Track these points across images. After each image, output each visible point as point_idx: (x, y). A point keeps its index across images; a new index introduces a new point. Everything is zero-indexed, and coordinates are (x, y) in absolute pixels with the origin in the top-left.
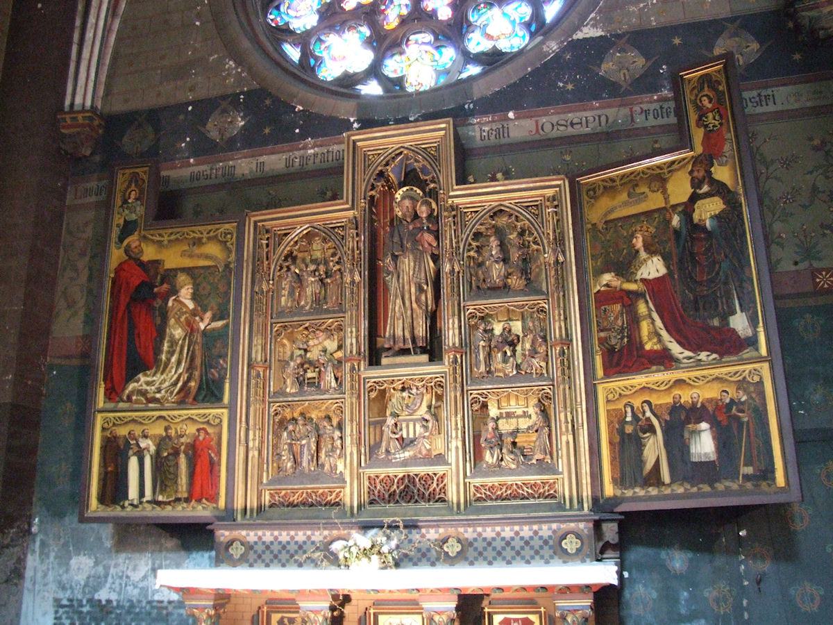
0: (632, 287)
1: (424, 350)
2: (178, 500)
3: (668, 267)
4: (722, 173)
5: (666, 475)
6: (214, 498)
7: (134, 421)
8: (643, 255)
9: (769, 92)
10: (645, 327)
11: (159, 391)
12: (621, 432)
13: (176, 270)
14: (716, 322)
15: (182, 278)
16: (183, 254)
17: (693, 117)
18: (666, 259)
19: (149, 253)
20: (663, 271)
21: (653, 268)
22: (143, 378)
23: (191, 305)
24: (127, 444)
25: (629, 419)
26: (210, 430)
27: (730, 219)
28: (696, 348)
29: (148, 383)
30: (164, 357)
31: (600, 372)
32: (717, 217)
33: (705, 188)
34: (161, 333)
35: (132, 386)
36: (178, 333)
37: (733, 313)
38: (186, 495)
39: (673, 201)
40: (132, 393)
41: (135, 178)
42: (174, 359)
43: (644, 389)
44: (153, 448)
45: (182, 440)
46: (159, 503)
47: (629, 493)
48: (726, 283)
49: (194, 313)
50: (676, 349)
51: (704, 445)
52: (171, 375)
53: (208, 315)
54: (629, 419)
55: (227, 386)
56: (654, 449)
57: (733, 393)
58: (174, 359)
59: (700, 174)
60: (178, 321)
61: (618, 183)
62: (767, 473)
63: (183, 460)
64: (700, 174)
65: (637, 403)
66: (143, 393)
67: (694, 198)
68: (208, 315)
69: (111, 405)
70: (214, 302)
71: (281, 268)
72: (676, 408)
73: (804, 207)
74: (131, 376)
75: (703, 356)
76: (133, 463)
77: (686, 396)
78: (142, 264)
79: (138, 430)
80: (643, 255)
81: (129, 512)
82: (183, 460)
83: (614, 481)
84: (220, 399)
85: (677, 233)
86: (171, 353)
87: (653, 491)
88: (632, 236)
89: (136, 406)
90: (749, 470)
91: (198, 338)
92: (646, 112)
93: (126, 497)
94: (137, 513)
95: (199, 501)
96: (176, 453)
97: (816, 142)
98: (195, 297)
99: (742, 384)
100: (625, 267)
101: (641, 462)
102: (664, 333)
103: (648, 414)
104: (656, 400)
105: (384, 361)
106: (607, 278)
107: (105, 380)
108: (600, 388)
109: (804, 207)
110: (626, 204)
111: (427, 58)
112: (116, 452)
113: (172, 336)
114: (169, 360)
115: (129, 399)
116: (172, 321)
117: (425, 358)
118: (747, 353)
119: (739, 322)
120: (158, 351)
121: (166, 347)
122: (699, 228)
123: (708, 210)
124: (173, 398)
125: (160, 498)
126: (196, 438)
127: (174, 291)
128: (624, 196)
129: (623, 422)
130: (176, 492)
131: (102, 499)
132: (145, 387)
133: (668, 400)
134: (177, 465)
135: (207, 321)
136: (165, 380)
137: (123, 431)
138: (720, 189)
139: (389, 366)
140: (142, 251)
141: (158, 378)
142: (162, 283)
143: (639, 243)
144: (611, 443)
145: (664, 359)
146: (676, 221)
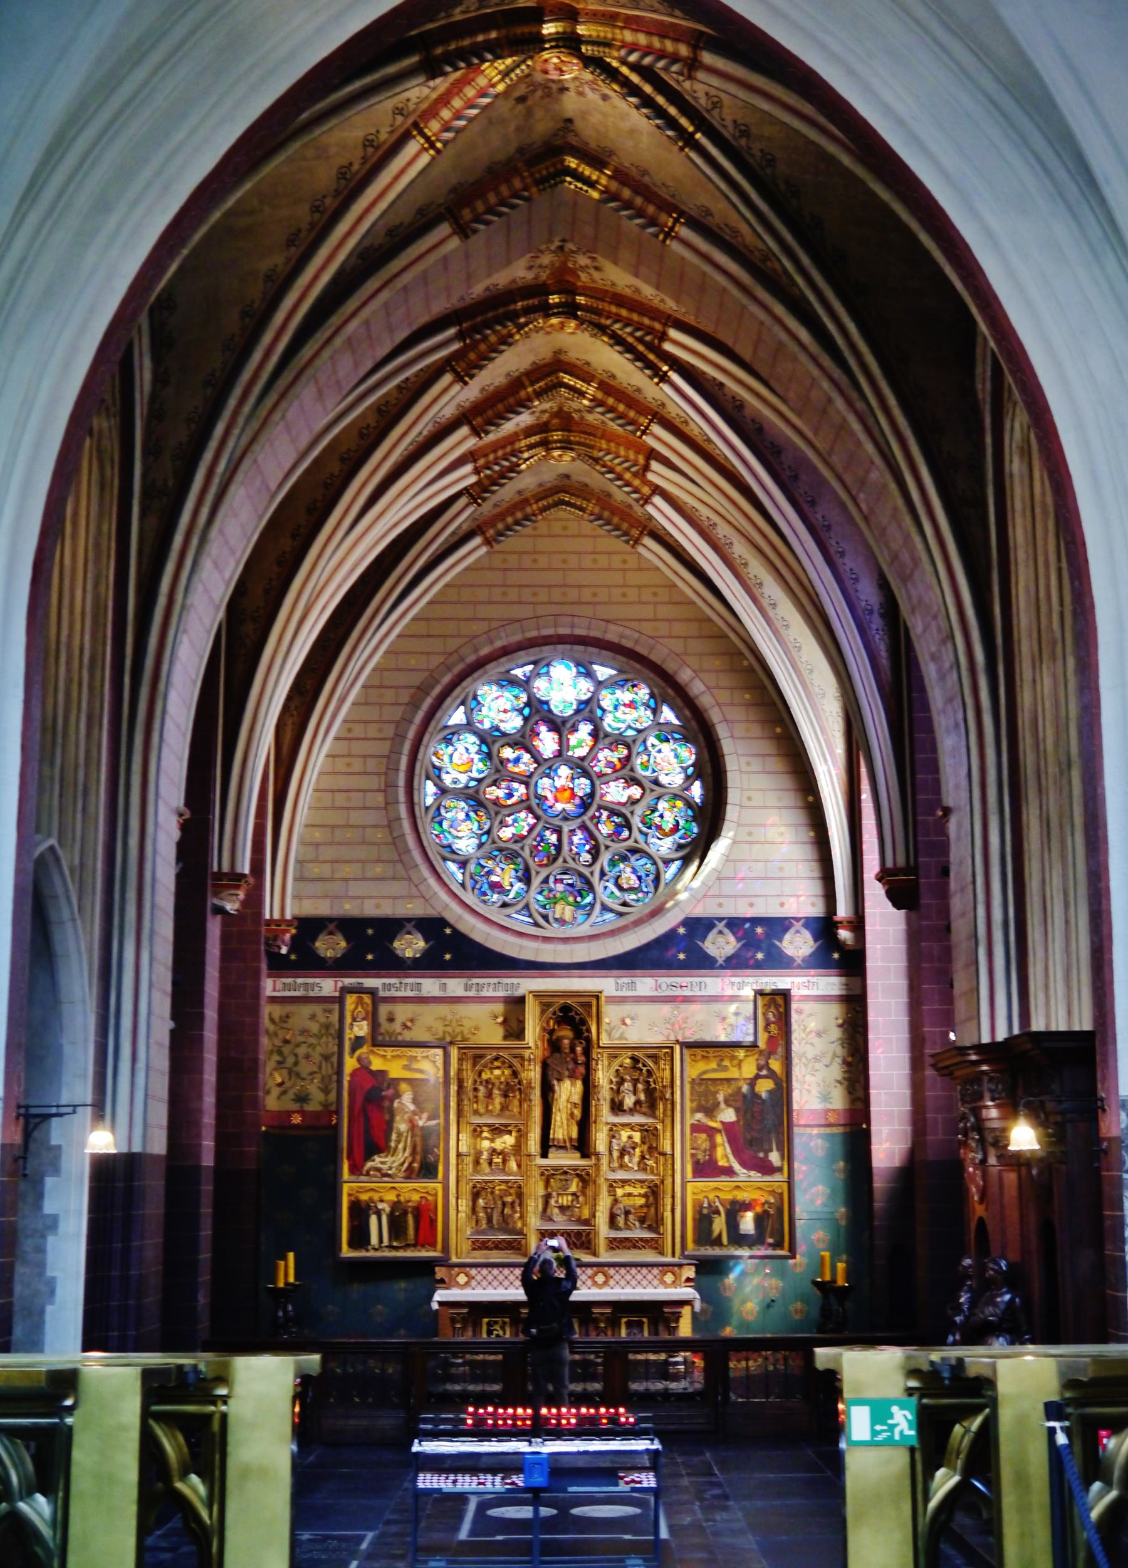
1: (576, 1148)
3: (737, 1116)
5: (725, 1240)
7: (372, 1190)
8: (722, 1105)
9: (815, 979)
10: (720, 1152)
11: (390, 1168)
12: (700, 1212)
13: (398, 1081)
14: (761, 1155)
15: (403, 1086)
16: (406, 1068)
18: (737, 1110)
19: (377, 1064)
21: (729, 1115)
22: (377, 1161)
23: (412, 1107)
24: (368, 1207)
25: (705, 1205)
26: (430, 1198)
29: (382, 1163)
30: (393, 1144)
32: (770, 1092)
33: (764, 1072)
35: (369, 1164)
37: (771, 1150)
38: (412, 1242)
41: (360, 1002)
42: (401, 1146)
43: (717, 1189)
44: (388, 1209)
45: (410, 1204)
48: (769, 1133)
49: (414, 1113)
52: (400, 1157)
53: (425, 1115)
54: (705, 1205)
56: (719, 1225)
58: (401, 1146)
59: (762, 1062)
61: (711, 1055)
65: (711, 1196)
66: (378, 1170)
67: (757, 1077)
68: (425, 1115)
69: (353, 1178)
71: (475, 1081)
72: (734, 1202)
73: (827, 1066)
74: (368, 1156)
76: (373, 1220)
78: (372, 1072)
79: (376, 1197)
80: (722, 1105)
81: (371, 1254)
84: (435, 1176)
85: (744, 1096)
86: (398, 1142)
88: (717, 1092)
89: (374, 1179)
92: (733, 984)
93: (368, 1242)
94: (378, 1254)
95: (423, 1246)
96: (405, 1213)
98: (415, 1101)
100: (710, 1110)
101: (710, 1231)
102: (731, 1157)
103: (718, 1204)
104: (723, 1196)
105: (550, 1155)
106: (699, 1116)
107: (349, 1158)
108: (689, 1184)
109: (827, 1066)
110: (714, 1070)
111: (571, 899)
112: (360, 1211)
113: (398, 1130)
114: (397, 1147)
120: (388, 1139)
121: (394, 1136)
122: (758, 1096)
124: (402, 1174)
125: (395, 1244)
126: (420, 1203)
127: (398, 1095)
128: (714, 1065)
129: (702, 1207)
130: (406, 1240)
131: (352, 1245)
132: (380, 1165)
133: (729, 1197)
134: (406, 1222)
135: (424, 1120)
136: (394, 1162)
137: (364, 1197)
138: (772, 1075)
140: (370, 1063)
141: (389, 1159)
142: (388, 1087)
143: (721, 1097)
144: (694, 1219)
145: (729, 1171)
146: (745, 1089)
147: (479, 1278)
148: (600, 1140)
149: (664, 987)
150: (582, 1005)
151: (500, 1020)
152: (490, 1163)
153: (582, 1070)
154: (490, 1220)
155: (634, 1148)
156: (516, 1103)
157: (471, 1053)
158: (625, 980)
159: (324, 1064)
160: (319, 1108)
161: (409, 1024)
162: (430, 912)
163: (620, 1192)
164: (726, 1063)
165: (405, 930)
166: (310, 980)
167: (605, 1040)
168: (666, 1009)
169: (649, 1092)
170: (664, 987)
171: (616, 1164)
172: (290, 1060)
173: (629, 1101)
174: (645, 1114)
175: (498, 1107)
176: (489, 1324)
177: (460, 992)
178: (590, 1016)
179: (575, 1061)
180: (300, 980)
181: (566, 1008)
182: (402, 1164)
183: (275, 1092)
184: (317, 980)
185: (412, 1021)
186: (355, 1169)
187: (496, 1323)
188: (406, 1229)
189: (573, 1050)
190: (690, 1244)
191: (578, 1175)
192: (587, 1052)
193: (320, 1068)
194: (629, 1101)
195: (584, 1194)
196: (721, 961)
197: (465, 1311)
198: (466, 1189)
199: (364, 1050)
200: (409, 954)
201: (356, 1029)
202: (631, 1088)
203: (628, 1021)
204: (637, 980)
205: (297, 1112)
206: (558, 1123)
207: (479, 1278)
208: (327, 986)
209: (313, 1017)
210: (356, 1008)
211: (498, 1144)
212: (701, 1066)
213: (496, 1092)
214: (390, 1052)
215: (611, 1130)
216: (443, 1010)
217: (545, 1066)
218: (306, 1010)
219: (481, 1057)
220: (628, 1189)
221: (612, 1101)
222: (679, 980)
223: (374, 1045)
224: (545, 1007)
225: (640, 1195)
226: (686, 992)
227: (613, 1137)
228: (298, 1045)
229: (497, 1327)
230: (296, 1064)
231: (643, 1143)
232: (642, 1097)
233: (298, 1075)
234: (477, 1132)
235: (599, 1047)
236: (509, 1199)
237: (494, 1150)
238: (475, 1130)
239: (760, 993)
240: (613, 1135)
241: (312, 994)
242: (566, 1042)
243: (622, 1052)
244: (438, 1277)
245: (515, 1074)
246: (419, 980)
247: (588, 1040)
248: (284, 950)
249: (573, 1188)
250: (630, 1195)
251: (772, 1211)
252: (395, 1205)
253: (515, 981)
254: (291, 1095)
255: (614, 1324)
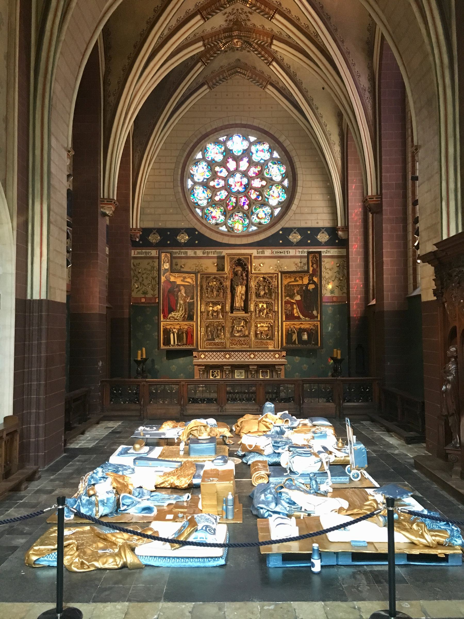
0: (293, 301)
1: (243, 310)
2: (184, 344)
4: (315, 279)
5: (297, 343)
6: (193, 344)
7: (171, 324)
8: (296, 294)
9: (329, 250)
10: (295, 310)
12: (288, 332)
13: (180, 285)
15: (182, 287)
16: (182, 280)
17: (311, 264)
18: (301, 296)
19: (172, 279)
20: (300, 299)
21: (298, 298)
23: (185, 295)
24: (170, 331)
27: (316, 289)
28: (306, 317)
29: (174, 315)
31: (284, 319)
33: (311, 282)
34: (177, 300)
35: (170, 315)
36: (182, 302)
39: (304, 283)
40: (170, 317)
41: (166, 256)
42: (181, 309)
43: (294, 324)
44: (177, 332)
46: (179, 345)
47: (289, 345)
49: (185, 297)
50: (301, 316)
51: (305, 337)
52: (181, 313)
55: (195, 317)
57: (312, 327)
58: (181, 309)
60: (181, 299)
62: (317, 344)
63: (184, 334)
64: (311, 278)
65: (292, 327)
66: (173, 317)
67: (309, 284)
68: (189, 298)
69: (164, 320)
70: (190, 295)
72: (300, 329)
74: (170, 312)
75: (307, 318)
76: (172, 335)
77: (302, 327)
79: (172, 327)
80: (296, 294)
81: (171, 347)
82: (184, 334)
83: (286, 343)
84: (193, 320)
85: (304, 290)
86: (180, 307)
87: (294, 346)
90: (314, 343)
91: (187, 304)
92: (299, 252)
94: (174, 347)
95: (189, 345)
96: (183, 333)
97: (338, 265)
98: (185, 293)
99: (314, 325)
100: (292, 296)
101: (292, 339)
102: (299, 313)
104: (296, 326)
105: (234, 312)
106: (287, 298)
110: (293, 282)
111: (241, 222)
112: (167, 332)
113: (180, 303)
114: (180, 309)
115: (170, 319)
116: (180, 299)
117: (244, 312)
118: (316, 319)
119: (315, 313)
120: (177, 306)
121: (178, 305)
122: (309, 290)
123: (311, 287)
124: (181, 319)
127: (180, 291)
128: (293, 280)
129: (289, 330)
131: (164, 344)
133: (299, 327)
134: (183, 336)
137: (168, 327)
138: (314, 283)
139: (235, 314)
140: (170, 278)
141: (177, 314)
142: (176, 288)
146: (304, 288)
147: (209, 356)
148: (252, 307)
149: (274, 252)
150: (245, 258)
151: (216, 264)
152: (213, 315)
153: (245, 282)
154: (212, 335)
155: (264, 310)
156: (222, 294)
157: (205, 276)
158: (261, 250)
159: (153, 280)
160: (151, 296)
161: (183, 266)
162: (190, 226)
163: (259, 325)
164: (297, 279)
165: (181, 233)
166: (147, 251)
167: (253, 271)
168: (275, 261)
169: (269, 290)
170: (274, 252)
171: (257, 316)
172: (141, 279)
173: (262, 293)
174: (268, 298)
175: (215, 295)
176: (212, 372)
177: (201, 255)
178: (248, 262)
179: (243, 279)
180: (143, 251)
181: (239, 260)
182: (182, 315)
183: (136, 290)
184: (150, 251)
185: (184, 265)
186: (164, 317)
187: (215, 371)
188: (183, 338)
189: (242, 275)
190: (284, 344)
191: (244, 320)
192: (247, 276)
193: (151, 282)
194: (262, 293)
195: (246, 327)
196: (295, 243)
197: (204, 367)
198: (203, 324)
199: (168, 274)
200: (182, 241)
201: (165, 266)
202: (263, 288)
203: (262, 265)
204: (265, 251)
205: (144, 298)
206: (237, 301)
207: (209, 356)
208: (154, 253)
209: (148, 264)
210: (165, 258)
211: (215, 309)
212: (289, 280)
213: (214, 290)
214: (177, 275)
215: (256, 303)
216: (195, 261)
217: (232, 280)
218: (146, 261)
219: (209, 277)
220: (262, 324)
221: (256, 293)
222: (280, 250)
223: (171, 272)
224: (231, 259)
225: (266, 326)
226: (283, 255)
227: (257, 306)
228: (143, 274)
229: (215, 373)
230: (143, 280)
231: (267, 308)
232: (267, 291)
233: (143, 284)
234: (207, 304)
235: (251, 273)
236: (219, 328)
237: (214, 311)
238: (207, 303)
239: (309, 253)
240: (256, 305)
241: (148, 255)
242: (239, 272)
243: (260, 275)
244: (194, 355)
245: (221, 283)
246: (186, 251)
247: (247, 271)
248: (137, 240)
249: (242, 324)
250: (262, 326)
251: (314, 332)
252: (179, 330)
253: (221, 251)
254: (141, 292)
255: (257, 372)
